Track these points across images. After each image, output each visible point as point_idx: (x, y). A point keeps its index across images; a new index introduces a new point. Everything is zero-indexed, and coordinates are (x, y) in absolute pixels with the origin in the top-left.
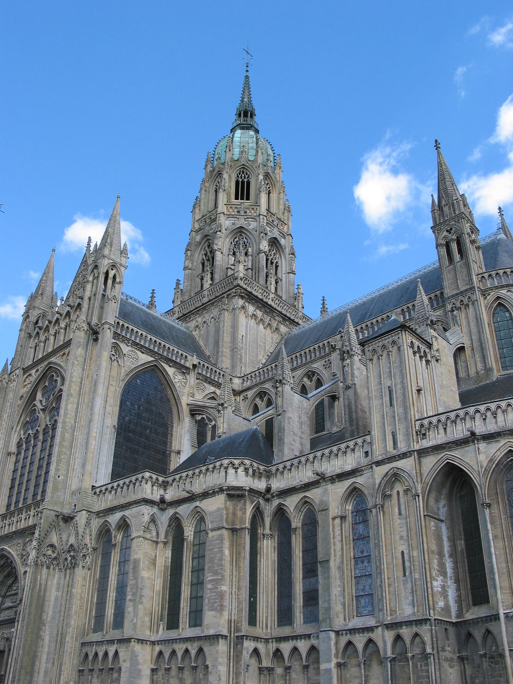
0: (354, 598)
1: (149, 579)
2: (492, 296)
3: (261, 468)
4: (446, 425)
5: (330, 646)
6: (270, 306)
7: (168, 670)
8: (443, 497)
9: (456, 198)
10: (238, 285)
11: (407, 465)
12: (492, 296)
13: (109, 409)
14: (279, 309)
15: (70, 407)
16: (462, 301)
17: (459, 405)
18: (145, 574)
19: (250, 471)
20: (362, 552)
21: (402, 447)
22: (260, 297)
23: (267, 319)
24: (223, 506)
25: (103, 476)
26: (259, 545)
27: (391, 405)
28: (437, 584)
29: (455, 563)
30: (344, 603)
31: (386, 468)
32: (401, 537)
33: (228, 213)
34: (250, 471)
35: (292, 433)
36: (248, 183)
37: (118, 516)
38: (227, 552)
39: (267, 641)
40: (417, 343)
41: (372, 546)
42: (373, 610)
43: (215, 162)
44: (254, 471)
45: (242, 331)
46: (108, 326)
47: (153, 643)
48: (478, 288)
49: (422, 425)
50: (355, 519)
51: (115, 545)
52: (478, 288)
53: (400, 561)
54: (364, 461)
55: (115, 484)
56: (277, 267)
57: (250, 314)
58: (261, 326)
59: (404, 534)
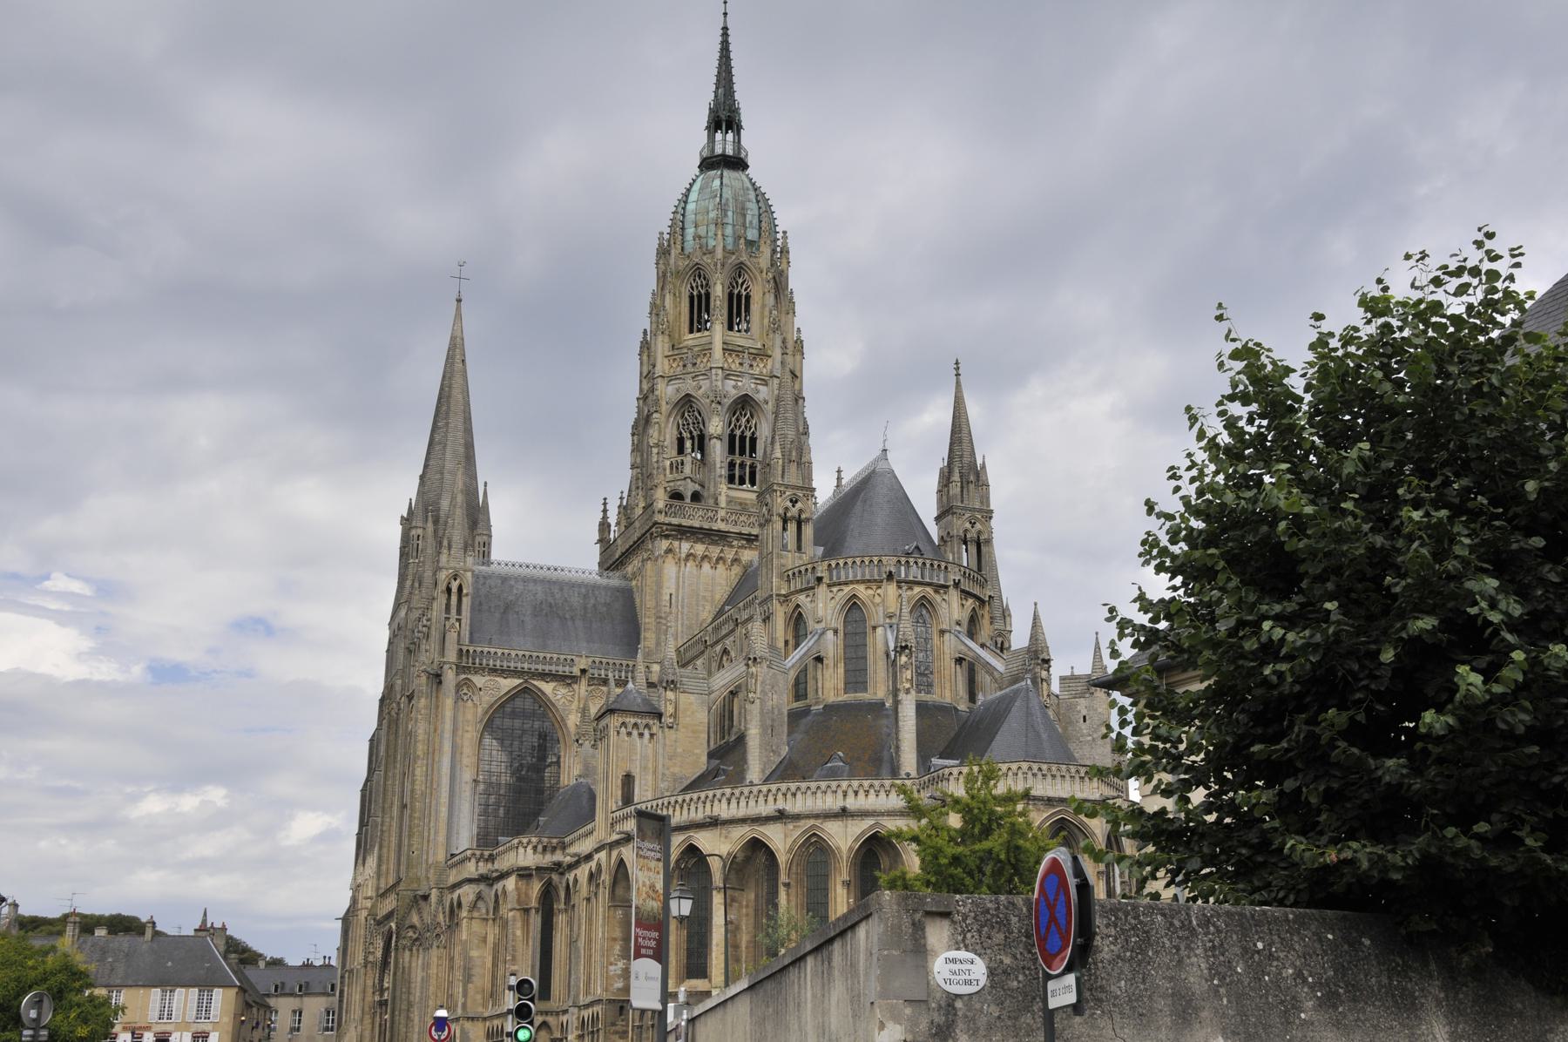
3: (555, 841)
10: (656, 523)
11: (603, 855)
13: (466, 761)
15: (418, 772)
18: (474, 953)
19: (540, 848)
22: (697, 524)
23: (715, 551)
25: (465, 839)
36: (708, 295)
38: (519, 933)
39: (557, 1014)
45: (669, 587)
47: (485, 1019)
56: (753, 440)
58: (706, 566)
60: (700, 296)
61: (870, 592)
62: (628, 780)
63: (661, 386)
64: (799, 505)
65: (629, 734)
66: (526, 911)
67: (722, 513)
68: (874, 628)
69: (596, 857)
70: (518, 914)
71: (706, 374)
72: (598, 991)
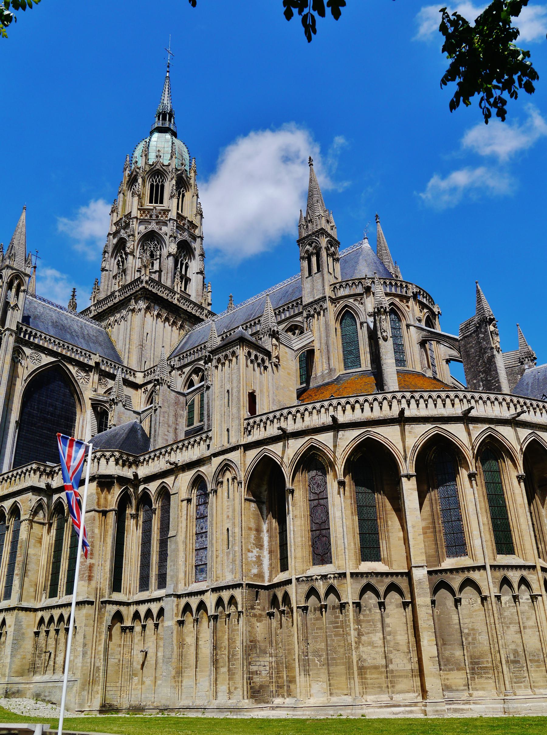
0: (194, 567)
1: (35, 555)
2: (342, 303)
4: (266, 424)
5: (172, 607)
6: (176, 305)
7: (47, 632)
8: (265, 483)
9: (318, 214)
11: (234, 456)
12: (342, 303)
14: (185, 307)
16: (315, 309)
17: (296, 402)
18: (31, 551)
19: (121, 462)
20: (202, 529)
21: (234, 442)
24: (95, 491)
26: (126, 523)
27: (228, 406)
28: (252, 556)
29: (270, 537)
30: (186, 571)
31: (221, 458)
32: (228, 517)
33: (142, 218)
34: (121, 462)
35: (166, 425)
36: (163, 187)
37: (11, 501)
38: (97, 531)
39: (128, 604)
40: (254, 353)
41: (208, 523)
42: (206, 578)
43: (133, 166)
44: (123, 461)
45: (148, 329)
46: (9, 332)
48: (329, 297)
49: (248, 424)
50: (199, 501)
51: (8, 528)
52: (329, 297)
53: (226, 536)
54: (208, 453)
55: (15, 472)
56: (187, 267)
57: (156, 313)
58: (167, 323)
59: (230, 514)
60: (157, 186)
61: (402, 304)
62: (252, 397)
63: (134, 224)
64: (333, 248)
65: (252, 362)
66: (104, 513)
67: (177, 296)
68: (408, 326)
69: (216, 461)
70: (97, 513)
71: (165, 224)
72: (229, 579)
